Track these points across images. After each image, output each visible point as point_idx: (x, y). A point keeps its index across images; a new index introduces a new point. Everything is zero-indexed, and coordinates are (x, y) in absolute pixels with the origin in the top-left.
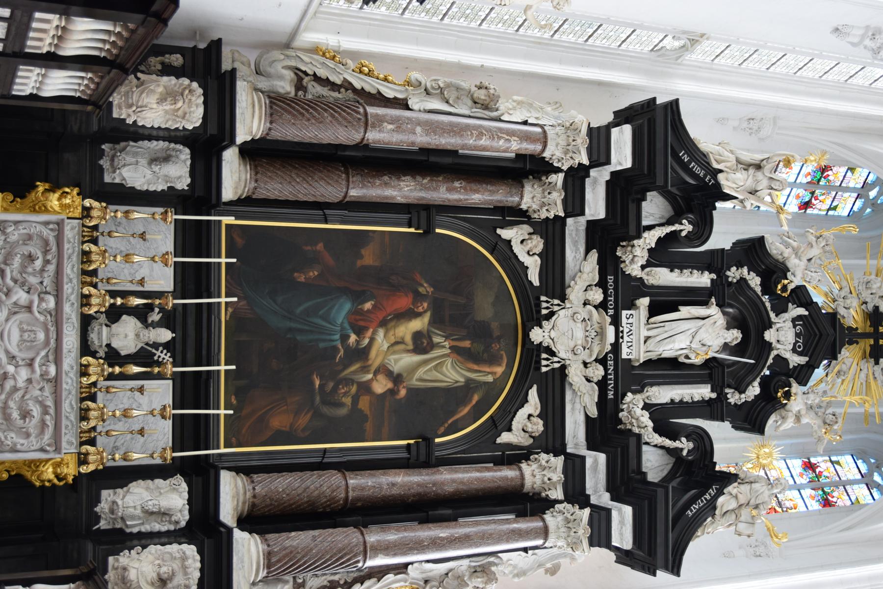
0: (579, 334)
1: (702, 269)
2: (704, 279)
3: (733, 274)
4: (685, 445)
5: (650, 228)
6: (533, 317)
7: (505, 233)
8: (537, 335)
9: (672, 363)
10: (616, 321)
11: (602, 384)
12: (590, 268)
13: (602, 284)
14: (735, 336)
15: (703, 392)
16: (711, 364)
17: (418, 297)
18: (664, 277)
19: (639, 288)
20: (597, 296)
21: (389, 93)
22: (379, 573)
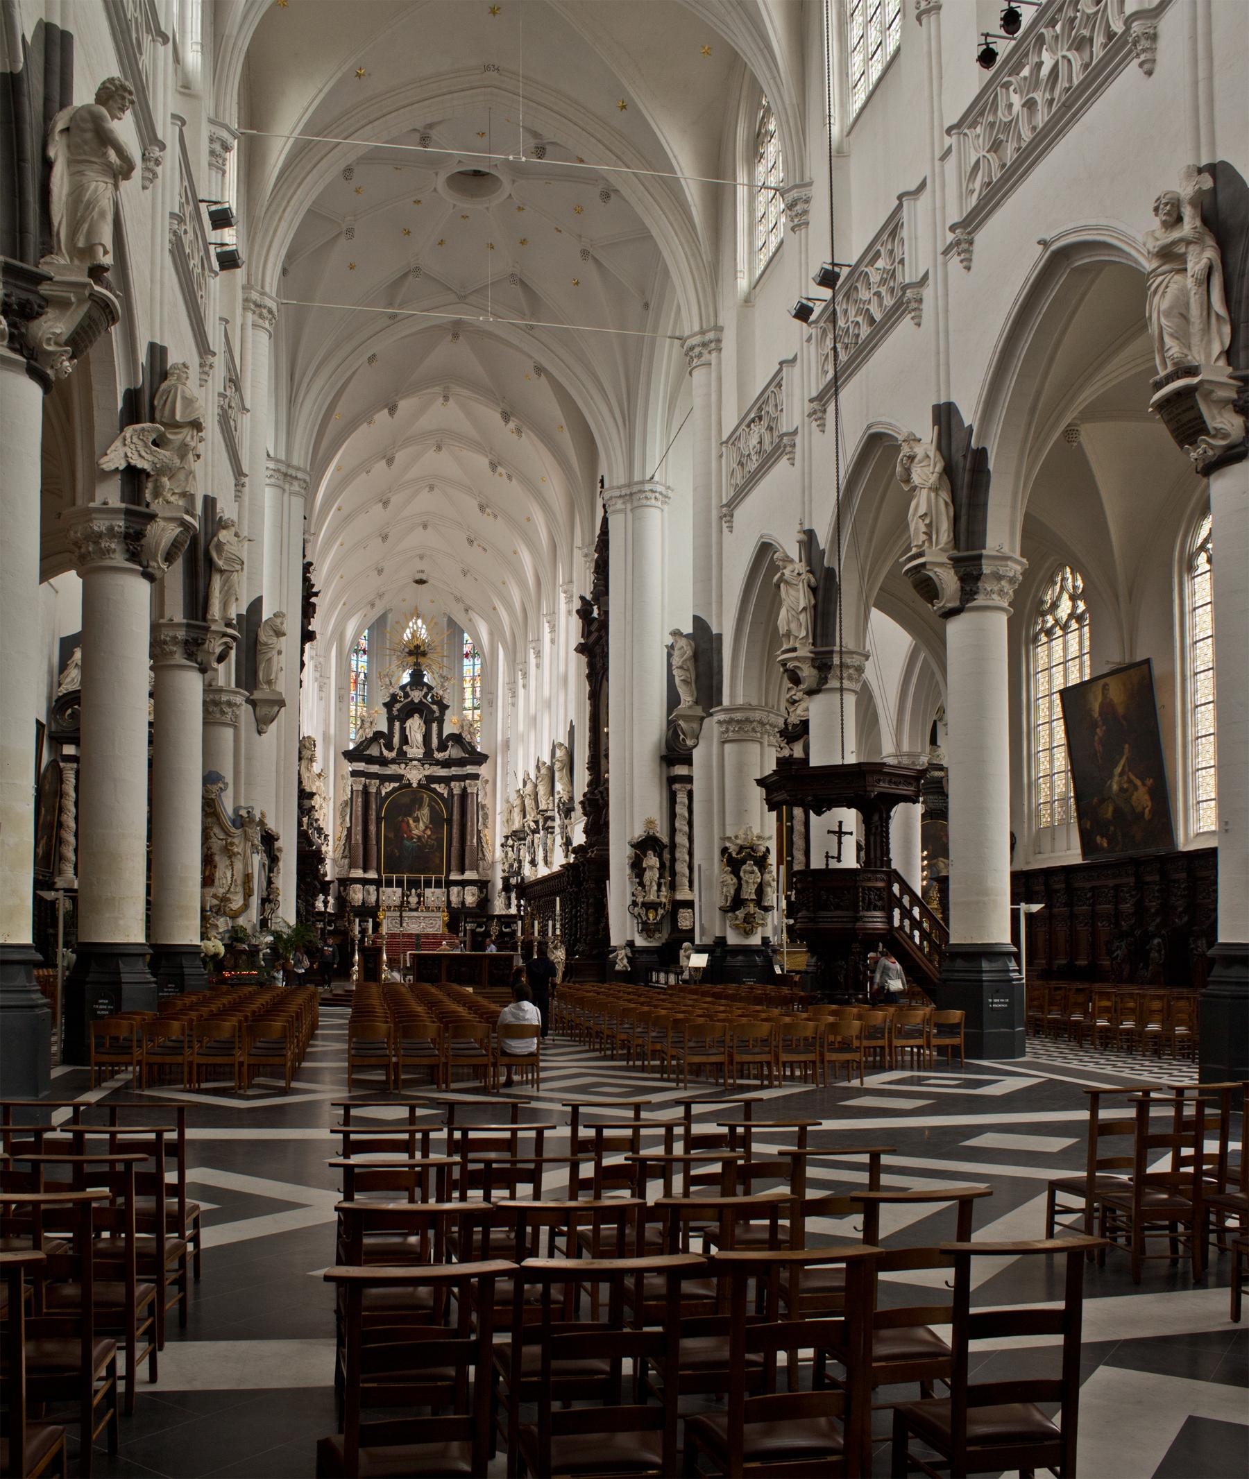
0: (415, 772)
1: (394, 725)
2: (397, 724)
3: (395, 713)
4: (450, 743)
5: (381, 753)
6: (410, 785)
7: (383, 794)
8: (415, 785)
9: (424, 737)
10: (411, 760)
11: (431, 765)
12: (394, 767)
13: (399, 764)
14: (416, 716)
15: (435, 726)
16: (425, 723)
17: (403, 821)
18: (396, 740)
19: (400, 749)
20: (403, 766)
21: (345, 833)
22: (479, 838)
